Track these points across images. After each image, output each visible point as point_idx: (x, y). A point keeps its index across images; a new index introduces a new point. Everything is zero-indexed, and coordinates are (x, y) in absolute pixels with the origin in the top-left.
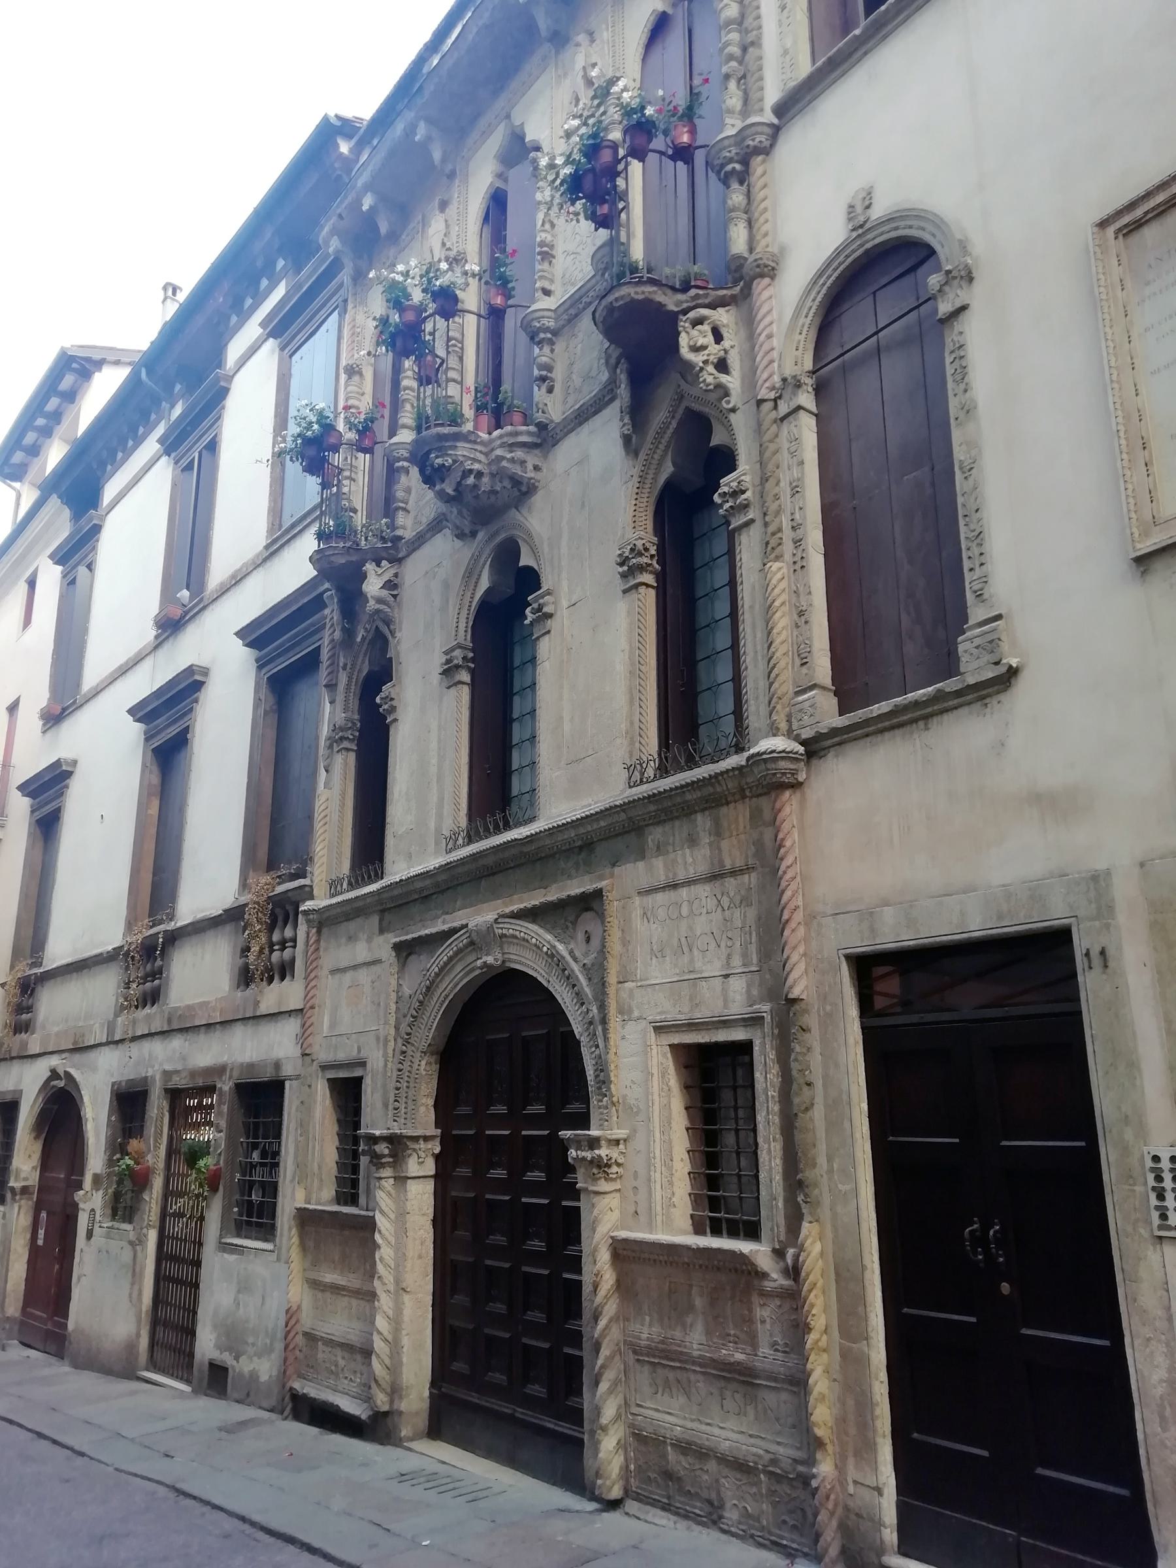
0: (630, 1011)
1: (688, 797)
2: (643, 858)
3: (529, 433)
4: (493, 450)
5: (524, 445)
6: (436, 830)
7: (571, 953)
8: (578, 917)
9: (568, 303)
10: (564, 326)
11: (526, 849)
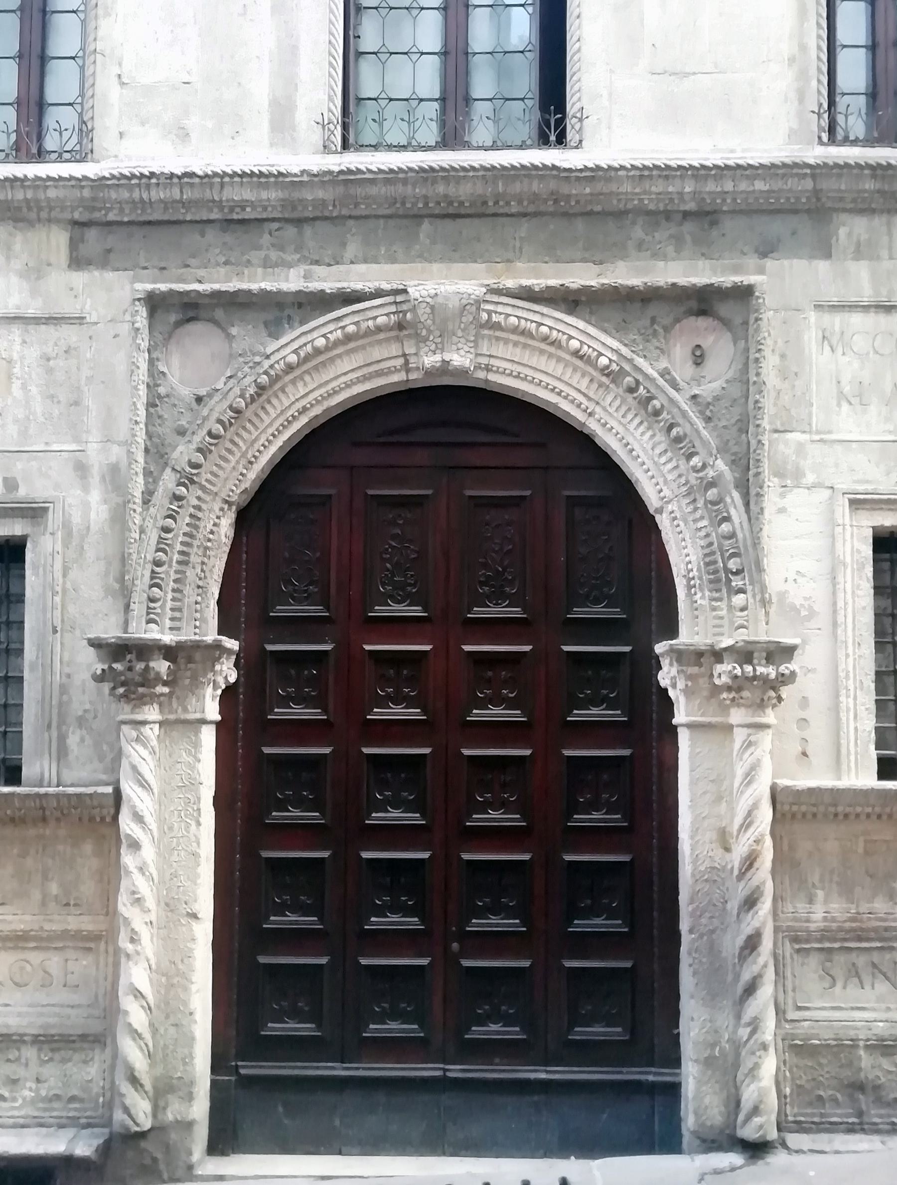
2: (828, 256)
7: (664, 373)
8: (678, 320)
11: (565, 189)
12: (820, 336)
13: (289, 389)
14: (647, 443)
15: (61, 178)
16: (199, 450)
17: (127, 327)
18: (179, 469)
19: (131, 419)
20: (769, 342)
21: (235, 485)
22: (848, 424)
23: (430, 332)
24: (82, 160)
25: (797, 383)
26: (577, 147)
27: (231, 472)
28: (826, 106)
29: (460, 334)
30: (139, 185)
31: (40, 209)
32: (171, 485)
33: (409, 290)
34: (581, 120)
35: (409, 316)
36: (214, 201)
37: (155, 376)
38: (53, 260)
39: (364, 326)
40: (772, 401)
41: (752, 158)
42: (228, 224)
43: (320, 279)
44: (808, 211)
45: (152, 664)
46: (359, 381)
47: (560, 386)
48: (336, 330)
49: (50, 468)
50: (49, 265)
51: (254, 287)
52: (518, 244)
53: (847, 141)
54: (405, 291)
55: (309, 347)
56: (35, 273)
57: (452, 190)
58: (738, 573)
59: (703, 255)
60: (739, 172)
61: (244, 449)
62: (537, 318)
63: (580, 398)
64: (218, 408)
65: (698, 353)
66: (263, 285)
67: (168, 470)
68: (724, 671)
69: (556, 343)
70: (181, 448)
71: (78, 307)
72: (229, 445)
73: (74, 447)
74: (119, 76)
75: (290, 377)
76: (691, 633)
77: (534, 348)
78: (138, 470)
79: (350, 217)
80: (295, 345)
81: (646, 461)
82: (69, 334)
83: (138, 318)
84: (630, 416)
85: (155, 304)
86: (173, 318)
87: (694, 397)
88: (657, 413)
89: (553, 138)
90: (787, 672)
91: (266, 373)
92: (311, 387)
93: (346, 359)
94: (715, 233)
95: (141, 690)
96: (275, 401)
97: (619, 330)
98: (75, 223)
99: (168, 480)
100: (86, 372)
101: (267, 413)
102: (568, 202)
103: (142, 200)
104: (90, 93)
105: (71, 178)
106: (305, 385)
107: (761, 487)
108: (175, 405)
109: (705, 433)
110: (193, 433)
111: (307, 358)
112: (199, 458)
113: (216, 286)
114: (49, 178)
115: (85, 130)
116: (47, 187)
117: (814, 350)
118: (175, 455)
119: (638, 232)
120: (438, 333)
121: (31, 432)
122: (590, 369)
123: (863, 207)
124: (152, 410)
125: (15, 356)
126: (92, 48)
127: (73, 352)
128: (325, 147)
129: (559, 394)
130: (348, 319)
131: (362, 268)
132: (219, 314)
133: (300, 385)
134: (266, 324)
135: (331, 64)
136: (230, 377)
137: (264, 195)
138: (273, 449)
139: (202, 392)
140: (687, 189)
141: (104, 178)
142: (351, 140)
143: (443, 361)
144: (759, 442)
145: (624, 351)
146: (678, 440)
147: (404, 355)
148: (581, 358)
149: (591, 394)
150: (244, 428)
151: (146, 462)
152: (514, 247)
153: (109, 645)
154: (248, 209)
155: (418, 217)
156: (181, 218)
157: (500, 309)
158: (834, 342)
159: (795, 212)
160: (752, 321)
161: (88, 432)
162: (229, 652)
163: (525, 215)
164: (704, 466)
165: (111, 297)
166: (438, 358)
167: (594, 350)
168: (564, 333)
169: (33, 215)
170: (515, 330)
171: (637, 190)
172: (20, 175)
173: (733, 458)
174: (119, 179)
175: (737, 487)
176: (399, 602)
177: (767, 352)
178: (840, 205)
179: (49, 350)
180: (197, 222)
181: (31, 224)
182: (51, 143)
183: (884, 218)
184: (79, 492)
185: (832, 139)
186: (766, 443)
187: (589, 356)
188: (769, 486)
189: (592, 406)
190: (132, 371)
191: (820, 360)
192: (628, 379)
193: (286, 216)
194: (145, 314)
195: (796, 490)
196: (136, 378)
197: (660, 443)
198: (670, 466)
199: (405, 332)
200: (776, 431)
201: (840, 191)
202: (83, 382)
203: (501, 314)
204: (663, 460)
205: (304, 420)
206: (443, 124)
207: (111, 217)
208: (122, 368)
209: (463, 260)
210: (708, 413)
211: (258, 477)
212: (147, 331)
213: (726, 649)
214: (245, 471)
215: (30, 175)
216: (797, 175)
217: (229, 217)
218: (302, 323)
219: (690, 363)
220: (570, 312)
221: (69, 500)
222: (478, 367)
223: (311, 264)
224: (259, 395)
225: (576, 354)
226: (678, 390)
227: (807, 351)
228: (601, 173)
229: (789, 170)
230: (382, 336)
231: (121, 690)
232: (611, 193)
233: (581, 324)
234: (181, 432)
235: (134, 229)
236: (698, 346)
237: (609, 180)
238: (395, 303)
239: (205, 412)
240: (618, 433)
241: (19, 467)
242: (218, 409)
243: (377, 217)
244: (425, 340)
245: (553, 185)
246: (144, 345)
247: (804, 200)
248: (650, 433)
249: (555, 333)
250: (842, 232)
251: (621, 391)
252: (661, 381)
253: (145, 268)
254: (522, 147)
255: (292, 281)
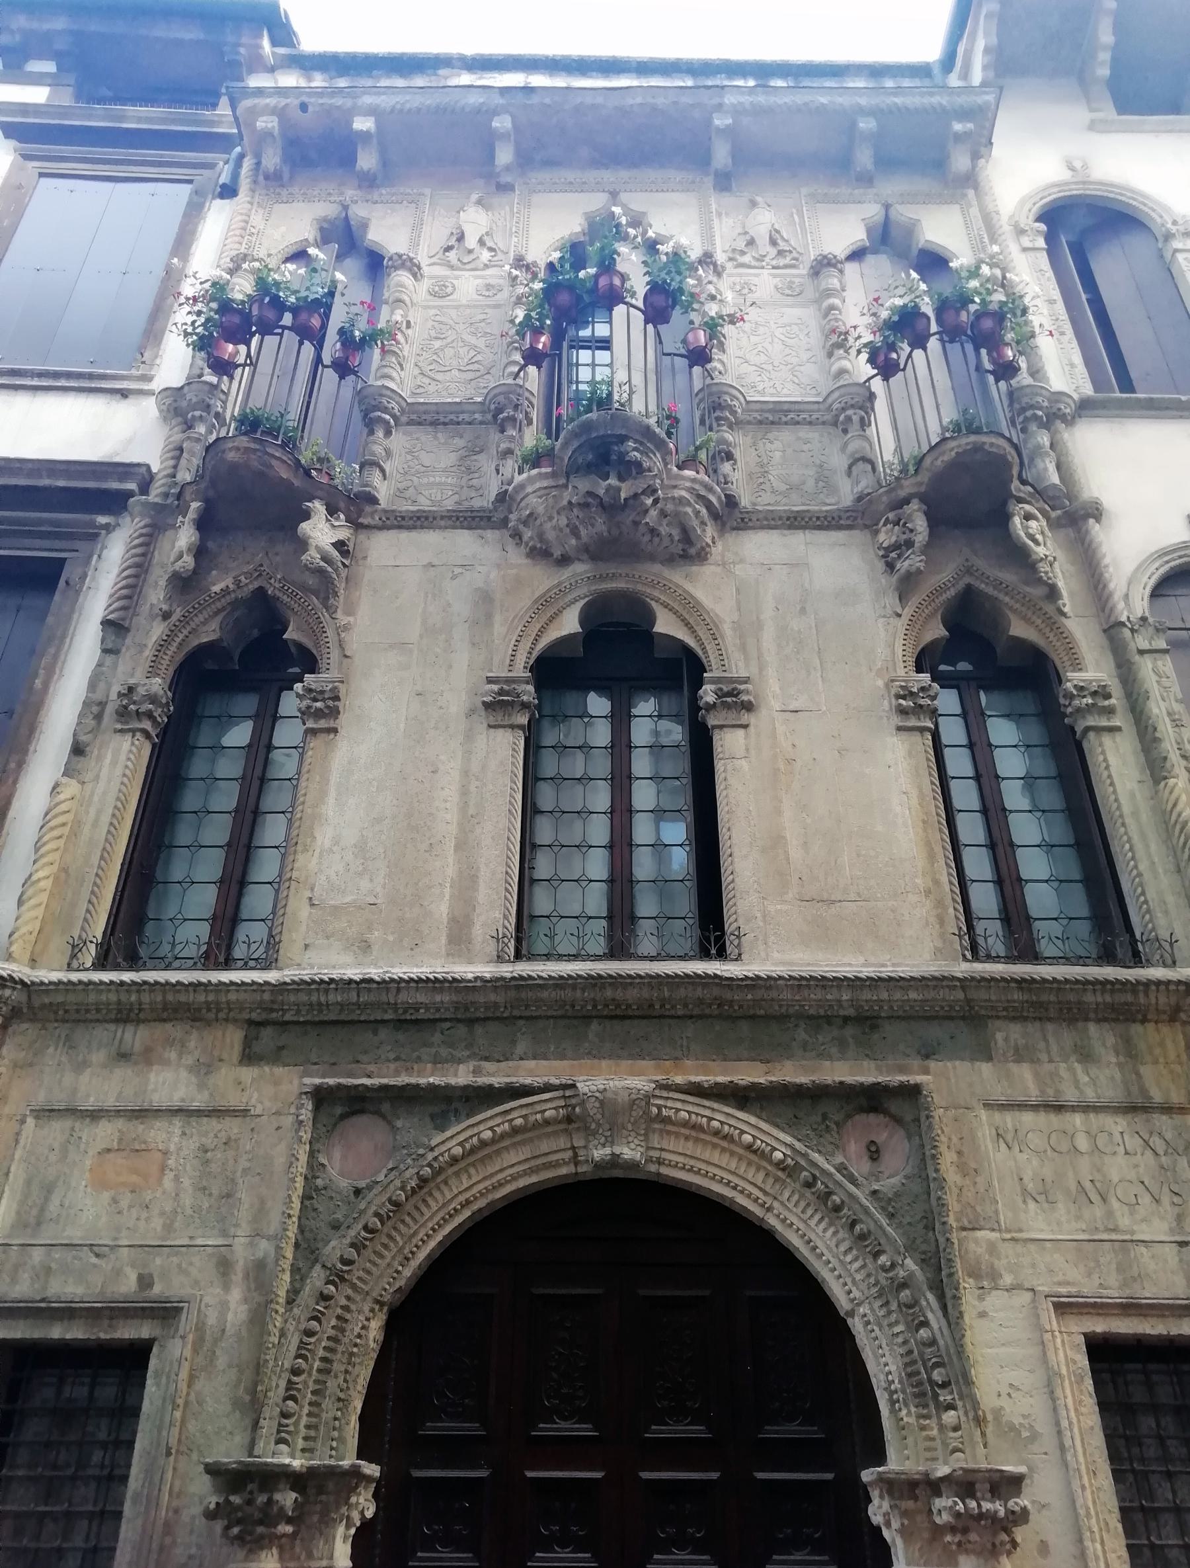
0: (994, 1276)
1: (1089, 998)
2: (989, 1058)
3: (719, 498)
4: (675, 487)
5: (709, 505)
6: (453, 920)
7: (841, 1168)
8: (849, 1116)
9: (771, 406)
10: (749, 423)
11: (728, 995)
12: (994, 1132)
13: (453, 1182)
14: (830, 1240)
15: (243, 983)
16: (352, 1245)
17: (291, 1119)
18: (329, 1266)
19: (284, 1213)
20: (943, 1138)
21: (389, 1283)
22: (1037, 1223)
23: (599, 1125)
24: (267, 968)
25: (978, 1179)
26: (736, 960)
27: (385, 1269)
28: (965, 929)
29: (630, 1127)
30: (318, 990)
31: (219, 1010)
32: (319, 1283)
33: (578, 1085)
34: (738, 937)
35: (577, 1110)
36: (389, 1004)
37: (314, 1167)
38: (225, 1056)
39: (532, 1119)
40: (955, 1198)
41: (903, 972)
42: (400, 1024)
43: (489, 1074)
44: (963, 1018)
45: (277, 1496)
46: (525, 1173)
47: (735, 1180)
48: (503, 1123)
49: (191, 1264)
50: (221, 1060)
51: (422, 1081)
52: (685, 1043)
53: (989, 958)
54: (573, 1086)
55: (475, 1139)
56: (204, 1069)
57: (619, 994)
58: (945, 1385)
59: (867, 1055)
60: (891, 983)
61: (401, 1244)
62: (707, 1113)
63: (756, 1192)
64: (377, 1201)
65: (873, 1149)
66: (431, 1080)
67: (318, 1267)
68: (945, 1506)
69: (727, 1137)
70: (333, 1243)
71: (244, 1100)
72: (385, 1240)
73: (220, 1242)
74: (310, 899)
75: (455, 1168)
76: (900, 1460)
77: (705, 1142)
78: (285, 1266)
79: (521, 1018)
80: (461, 1138)
81: (831, 1259)
82: (232, 1126)
83: (303, 1111)
84: (810, 1212)
85: (321, 1097)
86: (339, 1110)
87: (875, 1192)
88: (837, 1209)
89: (713, 951)
90: (1017, 1509)
91: (430, 1165)
92: (474, 1180)
93: (512, 1152)
94: (876, 1036)
95: (260, 1530)
96: (437, 1194)
97: (789, 1126)
98: (251, 1023)
99: (317, 1277)
100: (243, 1163)
101: (428, 1206)
102: (731, 1006)
103: (320, 1004)
104: (281, 912)
105: (254, 983)
106: (470, 1177)
107: (957, 1289)
108: (331, 1198)
109: (889, 1229)
110: (348, 1227)
111: (473, 1151)
112: (352, 1253)
113: (385, 1081)
114: (232, 983)
115: (273, 943)
116: (229, 991)
117: (990, 1147)
118: (327, 1250)
119: (801, 1034)
120: (608, 1127)
121: (177, 1225)
122: (764, 1164)
123: (1017, 1015)
124: (307, 1203)
125: (172, 1148)
126: (288, 876)
127: (233, 1143)
128: (498, 957)
129: (735, 1188)
130: (516, 1112)
131: (532, 1064)
132: (386, 1107)
133: (464, 1178)
134: (433, 1117)
135: (506, 889)
136: (392, 1169)
137: (438, 998)
138: (432, 1244)
139: (362, 1184)
140: (845, 997)
141: (285, 983)
142: (524, 952)
143: (613, 1154)
144: (948, 1240)
145: (798, 1145)
146: (863, 1237)
147: (573, 1148)
148: (755, 1152)
149: (768, 1189)
150: (403, 1221)
151: (294, 1258)
152: (682, 1046)
153: (227, 1471)
154: (422, 1011)
155: (587, 1018)
156: (356, 1018)
157: (670, 1104)
158: (1009, 1137)
159: (951, 1018)
160: (923, 1119)
161: (236, 1225)
162: (368, 1479)
163: (691, 1017)
164: (893, 1266)
165: (276, 1093)
166: (608, 1151)
167: (767, 1144)
168: (736, 1128)
169: (211, 1015)
170: (685, 1124)
171: (797, 998)
172: (204, 980)
173: (923, 1257)
174: (298, 984)
175: (931, 1288)
176: (565, 1419)
177: (943, 1148)
178: (994, 1013)
179: (209, 1142)
180: (370, 1022)
181: (209, 1024)
182: (239, 952)
183: (1037, 1024)
184: (218, 1290)
185: (976, 957)
186: (955, 1241)
187: (763, 1151)
188: (965, 1288)
189: (769, 1201)
190: (291, 1163)
191: (998, 1157)
192: (805, 1173)
193: (459, 1016)
194: (310, 1107)
195: (994, 1293)
196: (294, 1170)
197: (844, 1240)
198: (856, 1265)
199: (576, 1126)
200: (964, 1229)
201: (989, 1000)
202: (239, 1174)
203: (671, 1108)
204: (849, 1258)
205: (467, 1213)
206: (610, 937)
207: (288, 1017)
208: (280, 1161)
209: (632, 1057)
210: (890, 1209)
211: (413, 1274)
212: (311, 1123)
213: (942, 1479)
214: (400, 1268)
215: (214, 981)
216: (948, 986)
217: (403, 1017)
218: (468, 1116)
219: (866, 1158)
220: (741, 1107)
221: (207, 1299)
222: (649, 1160)
223: (481, 1059)
224: (420, 1188)
225: (749, 1147)
226: (857, 1185)
227: (983, 1148)
228: (760, 982)
229: (939, 983)
230: (549, 1129)
231: (236, 1530)
232: (772, 1000)
233: (753, 1120)
234: (336, 1226)
235: (309, 1028)
236: (872, 1142)
237: (770, 988)
238: (564, 1097)
239: (362, 1206)
240: (798, 1229)
241: (158, 1262)
242: (377, 1201)
243: (548, 1018)
244: (594, 1133)
245: (716, 992)
246: (306, 1136)
247: (957, 1008)
248: (832, 1230)
249: (726, 1128)
250: (999, 1036)
251: (798, 1186)
252: (838, 1177)
253: (315, 1064)
254: (682, 958)
255: (461, 1076)
